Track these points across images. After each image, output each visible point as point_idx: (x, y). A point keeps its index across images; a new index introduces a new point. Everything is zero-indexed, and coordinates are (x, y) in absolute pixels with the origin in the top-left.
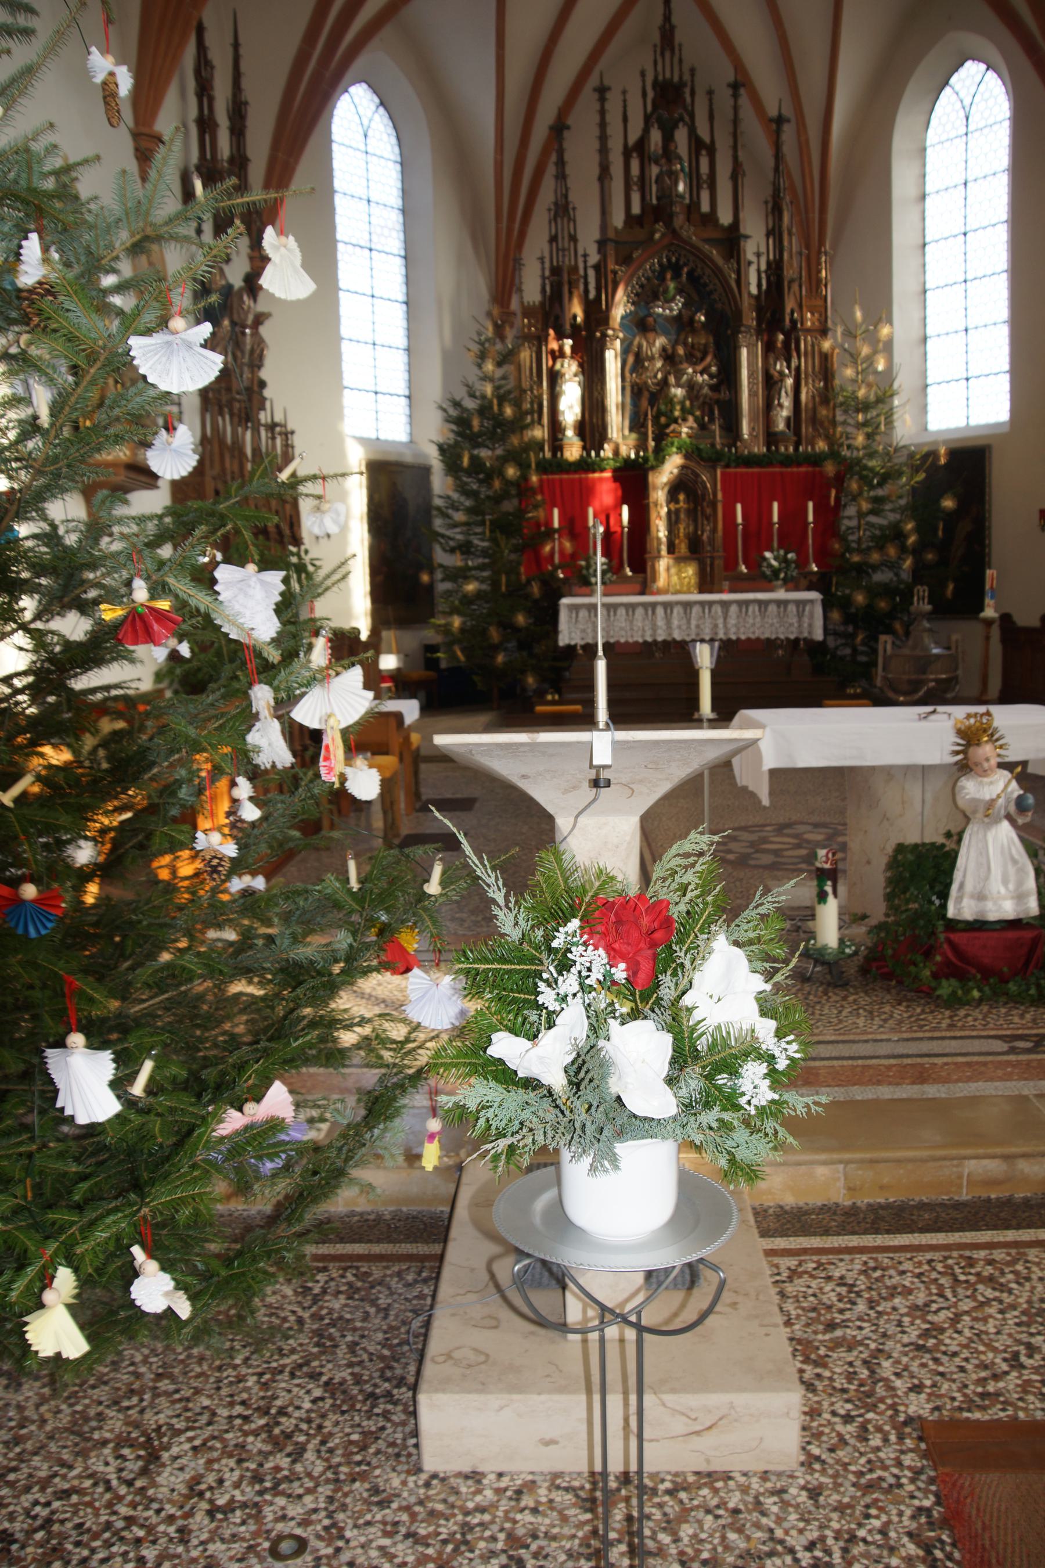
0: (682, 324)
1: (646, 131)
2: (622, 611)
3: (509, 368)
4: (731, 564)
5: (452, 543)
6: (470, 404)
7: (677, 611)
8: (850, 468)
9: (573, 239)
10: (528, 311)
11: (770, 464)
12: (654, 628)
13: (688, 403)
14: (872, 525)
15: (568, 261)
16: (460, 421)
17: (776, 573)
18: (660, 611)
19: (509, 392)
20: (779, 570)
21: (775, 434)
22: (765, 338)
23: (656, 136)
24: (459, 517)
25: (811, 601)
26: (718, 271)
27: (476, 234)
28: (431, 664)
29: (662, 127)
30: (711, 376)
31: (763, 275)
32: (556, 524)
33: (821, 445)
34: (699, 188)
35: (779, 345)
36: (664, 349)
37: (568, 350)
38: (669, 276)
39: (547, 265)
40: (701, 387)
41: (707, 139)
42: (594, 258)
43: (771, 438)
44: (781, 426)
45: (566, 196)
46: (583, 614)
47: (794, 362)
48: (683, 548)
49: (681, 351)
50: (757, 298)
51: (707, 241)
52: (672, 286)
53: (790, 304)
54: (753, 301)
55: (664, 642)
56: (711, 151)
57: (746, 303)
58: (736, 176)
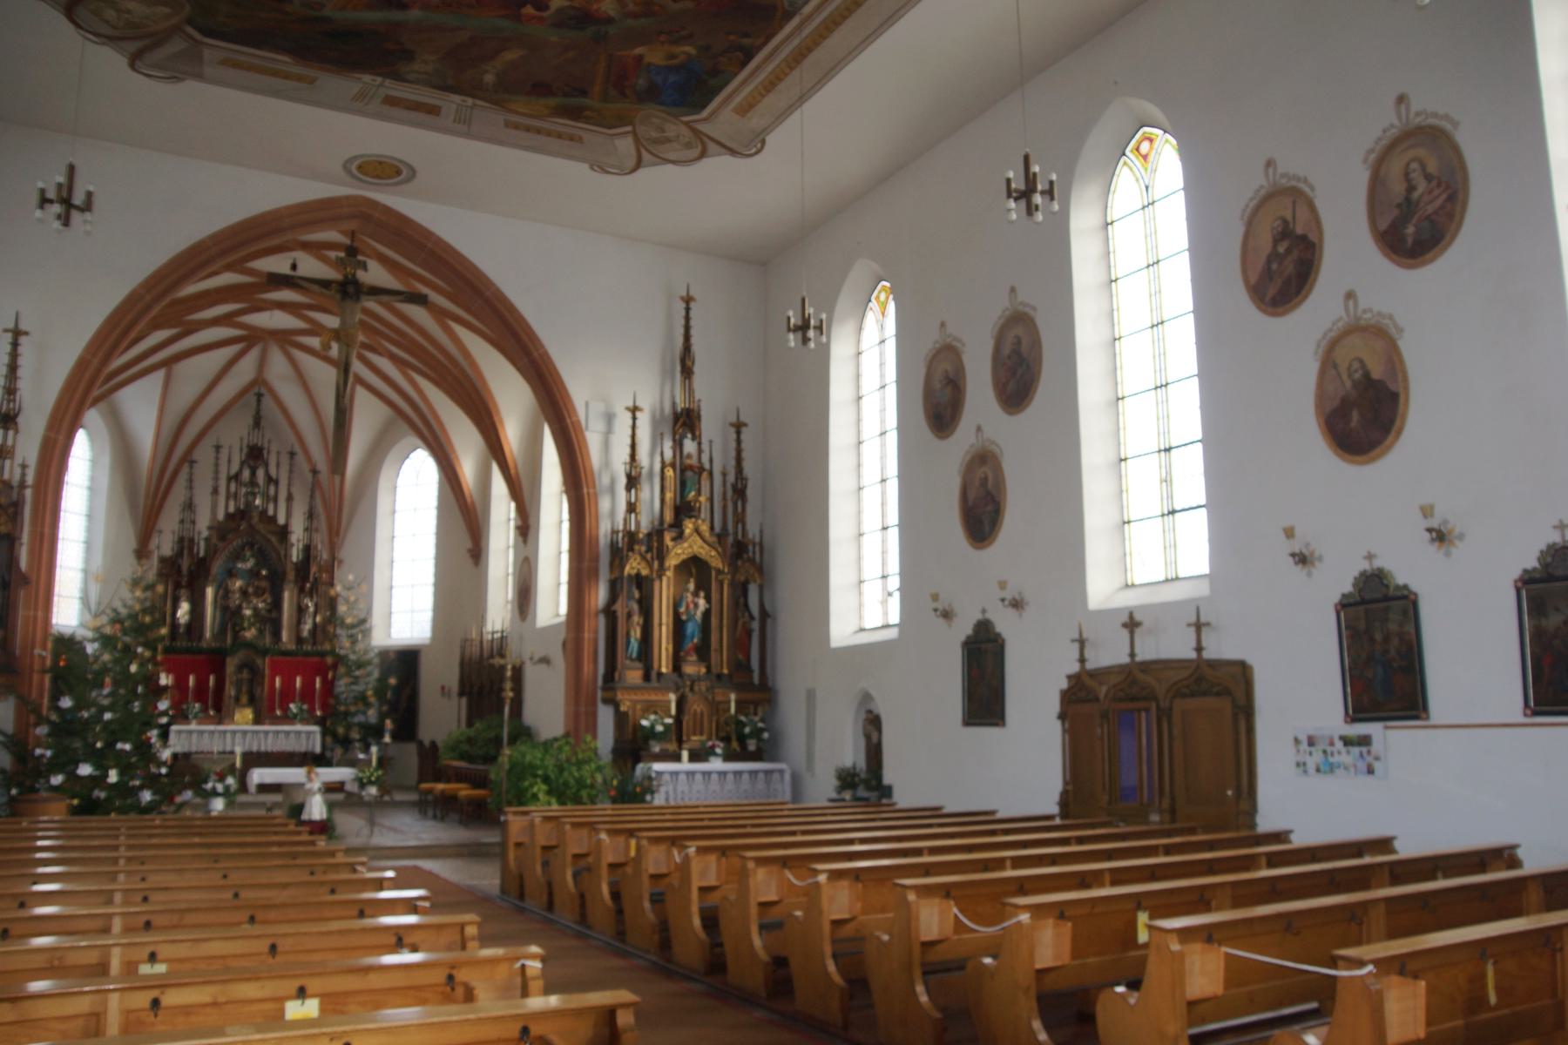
0: (253, 574)
2: (206, 735)
3: (149, 594)
4: (272, 709)
7: (238, 736)
8: (340, 660)
9: (193, 522)
10: (163, 560)
12: (225, 744)
13: (252, 620)
14: (353, 691)
15: (186, 534)
17: (295, 716)
18: (228, 735)
23: (246, 474)
25: (314, 732)
27: (133, 505)
29: (250, 466)
30: (268, 604)
33: (327, 647)
34: (268, 502)
36: (241, 588)
42: (205, 533)
43: (299, 640)
44: (305, 634)
47: (315, 599)
48: (244, 699)
50: (296, 564)
53: (313, 569)
56: (276, 482)
58: (290, 498)
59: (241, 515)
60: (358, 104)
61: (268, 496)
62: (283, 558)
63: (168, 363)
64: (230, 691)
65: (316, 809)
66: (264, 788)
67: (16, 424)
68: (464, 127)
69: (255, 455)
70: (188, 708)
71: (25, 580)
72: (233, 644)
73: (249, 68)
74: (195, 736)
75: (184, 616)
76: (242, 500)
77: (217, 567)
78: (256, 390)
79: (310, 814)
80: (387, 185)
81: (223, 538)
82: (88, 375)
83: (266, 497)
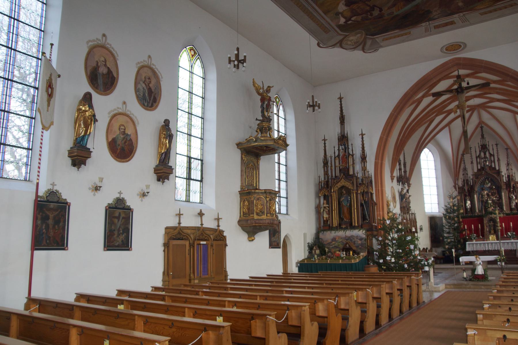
0: (490, 188)
1: (480, 153)
2: (479, 245)
5: (446, 232)
6: (448, 206)
7: (490, 244)
9: (467, 174)
11: (510, 215)
12: (485, 247)
13: (492, 204)
16: (446, 210)
17: (510, 236)
19: (456, 204)
20: (511, 236)
21: (512, 208)
22: (508, 189)
23: (482, 155)
24: (447, 227)
26: (496, 178)
28: (444, 254)
30: (497, 198)
31: (507, 178)
32: (466, 228)
34: (491, 163)
35: (512, 191)
36: (487, 193)
37: (467, 195)
38: (486, 180)
39: (462, 179)
40: (495, 200)
41: (492, 153)
42: (471, 177)
43: (511, 209)
44: (513, 207)
45: (465, 167)
46: (471, 245)
47: (515, 194)
48: (492, 232)
49: (490, 194)
51: (494, 173)
52: (487, 182)
53: (512, 184)
54: (504, 183)
55: (488, 250)
56: (493, 156)
57: (502, 184)
59: (483, 169)
60: (428, 32)
61: (491, 160)
62: (500, 181)
63: (448, 124)
64: (487, 229)
65: (480, 270)
66: (467, 263)
67: (366, 160)
68: (466, 23)
69: (484, 148)
70: (472, 236)
71: (376, 204)
72: (485, 213)
73: (391, 38)
74: (475, 245)
75: (469, 205)
76: (483, 163)
77: (477, 189)
78: (480, 126)
79: (478, 272)
80: (460, 51)
81: (477, 178)
82: (384, 141)
83: (491, 162)
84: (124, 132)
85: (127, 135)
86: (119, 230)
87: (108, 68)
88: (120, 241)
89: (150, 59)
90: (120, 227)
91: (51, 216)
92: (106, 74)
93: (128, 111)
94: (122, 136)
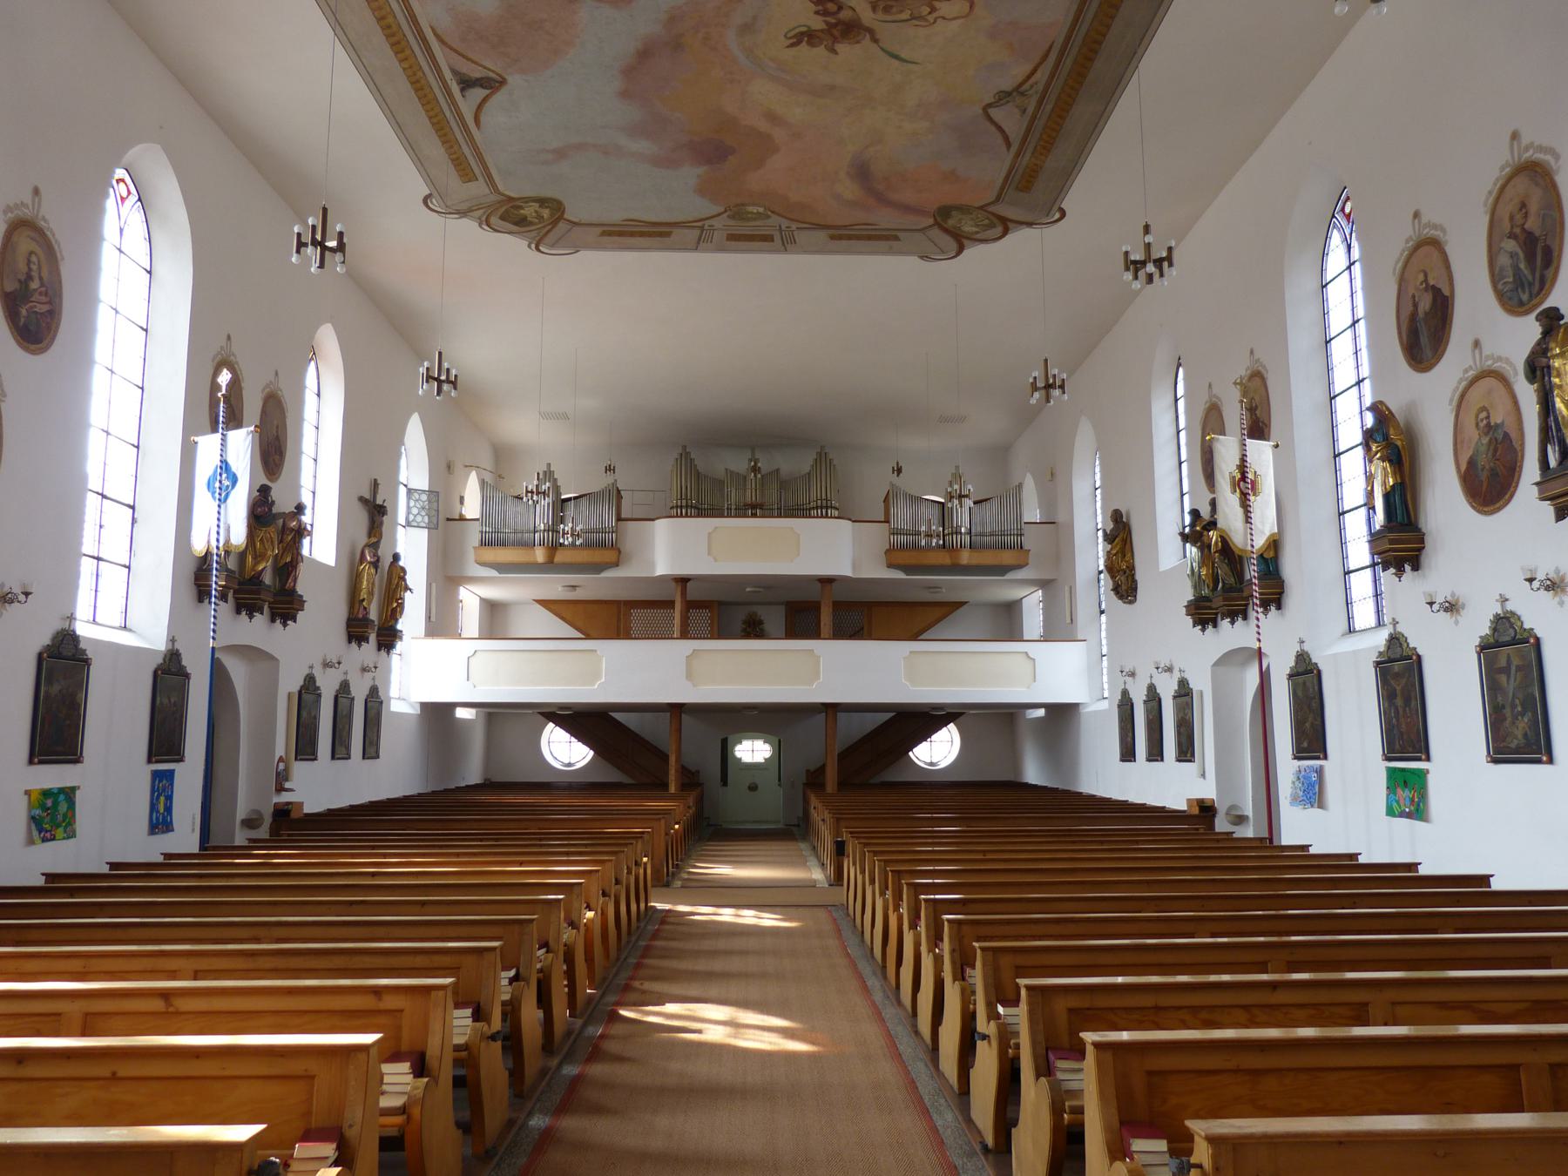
84: (1488, 425)
85: (1497, 426)
86: (1513, 706)
87: (1433, 287)
88: (1519, 734)
89: (1515, 143)
90: (1513, 698)
91: (1398, 688)
92: (1431, 309)
93: (1488, 358)
94: (1485, 440)
